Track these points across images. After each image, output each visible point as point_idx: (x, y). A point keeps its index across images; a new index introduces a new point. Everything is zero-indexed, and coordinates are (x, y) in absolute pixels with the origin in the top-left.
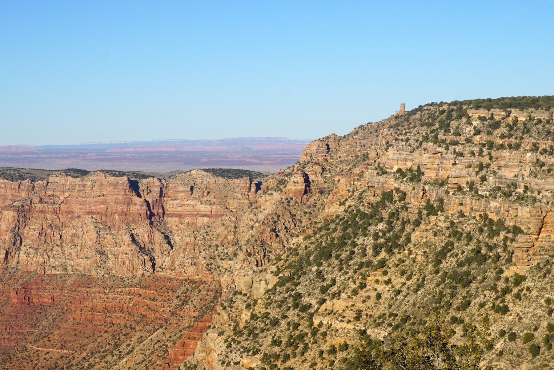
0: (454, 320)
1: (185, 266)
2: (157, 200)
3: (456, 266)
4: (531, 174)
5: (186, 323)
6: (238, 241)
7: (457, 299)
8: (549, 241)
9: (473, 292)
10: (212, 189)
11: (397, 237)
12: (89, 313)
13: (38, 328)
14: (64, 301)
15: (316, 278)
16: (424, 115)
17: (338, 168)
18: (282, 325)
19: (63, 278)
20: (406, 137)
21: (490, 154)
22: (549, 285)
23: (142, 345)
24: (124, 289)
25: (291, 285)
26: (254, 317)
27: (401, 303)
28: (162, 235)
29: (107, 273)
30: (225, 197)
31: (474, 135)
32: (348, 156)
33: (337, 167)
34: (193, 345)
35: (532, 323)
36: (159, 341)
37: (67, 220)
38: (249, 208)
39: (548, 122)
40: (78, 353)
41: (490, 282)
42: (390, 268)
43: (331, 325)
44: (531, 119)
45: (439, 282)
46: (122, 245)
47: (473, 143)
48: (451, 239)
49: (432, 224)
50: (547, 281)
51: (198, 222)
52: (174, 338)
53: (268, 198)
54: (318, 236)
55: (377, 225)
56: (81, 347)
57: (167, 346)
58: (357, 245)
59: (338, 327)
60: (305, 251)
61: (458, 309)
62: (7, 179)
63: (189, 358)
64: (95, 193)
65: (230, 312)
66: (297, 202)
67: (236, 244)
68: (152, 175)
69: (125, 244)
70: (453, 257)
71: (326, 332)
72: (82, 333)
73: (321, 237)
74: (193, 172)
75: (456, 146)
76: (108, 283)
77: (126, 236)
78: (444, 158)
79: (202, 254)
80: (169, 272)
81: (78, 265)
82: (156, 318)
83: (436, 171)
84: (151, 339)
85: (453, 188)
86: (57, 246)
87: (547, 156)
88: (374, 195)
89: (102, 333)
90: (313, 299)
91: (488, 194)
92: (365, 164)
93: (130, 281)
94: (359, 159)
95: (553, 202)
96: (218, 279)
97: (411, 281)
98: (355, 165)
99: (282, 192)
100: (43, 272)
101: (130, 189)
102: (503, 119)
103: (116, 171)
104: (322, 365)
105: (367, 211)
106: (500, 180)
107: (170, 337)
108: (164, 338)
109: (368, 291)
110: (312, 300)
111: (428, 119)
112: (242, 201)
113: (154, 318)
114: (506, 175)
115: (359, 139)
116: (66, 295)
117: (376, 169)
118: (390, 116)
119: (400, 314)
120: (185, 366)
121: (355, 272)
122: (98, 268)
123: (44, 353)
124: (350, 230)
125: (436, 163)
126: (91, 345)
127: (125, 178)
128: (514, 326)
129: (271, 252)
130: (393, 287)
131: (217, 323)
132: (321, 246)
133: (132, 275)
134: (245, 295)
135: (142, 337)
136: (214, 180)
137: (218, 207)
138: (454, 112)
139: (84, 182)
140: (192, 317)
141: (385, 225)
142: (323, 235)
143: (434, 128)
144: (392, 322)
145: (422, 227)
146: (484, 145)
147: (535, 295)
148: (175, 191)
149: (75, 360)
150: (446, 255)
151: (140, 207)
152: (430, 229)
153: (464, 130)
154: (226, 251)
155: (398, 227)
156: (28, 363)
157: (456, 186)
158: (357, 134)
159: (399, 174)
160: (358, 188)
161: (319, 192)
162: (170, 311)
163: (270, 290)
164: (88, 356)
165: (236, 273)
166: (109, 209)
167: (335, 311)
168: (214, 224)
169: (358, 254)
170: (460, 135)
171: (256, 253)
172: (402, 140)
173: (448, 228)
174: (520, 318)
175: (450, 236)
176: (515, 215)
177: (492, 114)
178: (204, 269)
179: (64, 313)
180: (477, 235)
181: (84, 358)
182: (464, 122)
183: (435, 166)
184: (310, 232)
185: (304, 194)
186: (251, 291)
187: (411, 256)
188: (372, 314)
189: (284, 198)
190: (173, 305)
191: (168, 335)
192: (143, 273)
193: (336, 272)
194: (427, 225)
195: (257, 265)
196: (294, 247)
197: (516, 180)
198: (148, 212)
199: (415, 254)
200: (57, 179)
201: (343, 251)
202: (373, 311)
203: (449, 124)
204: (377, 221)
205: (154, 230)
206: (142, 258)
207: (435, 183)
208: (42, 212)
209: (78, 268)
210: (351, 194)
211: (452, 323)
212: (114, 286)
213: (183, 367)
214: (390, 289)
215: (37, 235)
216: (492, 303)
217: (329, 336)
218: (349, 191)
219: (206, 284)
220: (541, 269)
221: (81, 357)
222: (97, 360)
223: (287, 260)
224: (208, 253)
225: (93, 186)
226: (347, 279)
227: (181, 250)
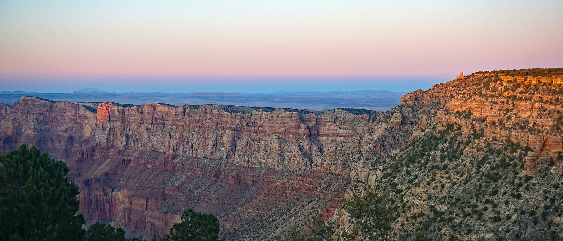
0: (488, 201)
1: (329, 165)
4: (538, 116)
5: (329, 197)
6: (361, 151)
7: (490, 189)
8: (547, 156)
9: (500, 184)
11: (456, 152)
13: (244, 198)
19: (259, 170)
20: (463, 92)
21: (513, 103)
22: (546, 182)
23: (303, 209)
27: (456, 190)
31: (504, 91)
33: (421, 109)
36: (313, 208)
38: (368, 132)
39: (550, 84)
40: (267, 213)
42: (450, 170)
44: (540, 82)
45: (479, 178)
46: (294, 152)
47: (503, 96)
48: (488, 153)
49: (476, 144)
50: (545, 180)
51: (338, 140)
53: (379, 126)
54: (408, 149)
57: (318, 211)
58: (431, 156)
59: (418, 203)
61: (490, 195)
62: (228, 112)
63: (330, 218)
66: (396, 129)
70: (488, 164)
71: (410, 206)
72: (269, 202)
73: (410, 150)
74: (336, 110)
75: (493, 98)
76: (285, 173)
77: (296, 147)
80: (321, 168)
81: (268, 163)
82: (312, 195)
83: (480, 113)
84: (309, 207)
85: (490, 123)
86: (256, 151)
88: (442, 126)
89: (281, 202)
94: (435, 105)
97: (462, 177)
99: (388, 123)
100: (248, 166)
102: (523, 82)
103: (291, 109)
105: (438, 135)
106: (519, 119)
107: (320, 206)
108: (316, 206)
109: (436, 182)
111: (477, 81)
115: (435, 93)
117: (444, 111)
118: (454, 79)
119: (455, 196)
120: (328, 223)
121: (429, 172)
123: (247, 213)
124: (427, 147)
125: (480, 108)
130: (451, 181)
135: (303, 205)
136: (348, 115)
137: (350, 131)
139: (272, 115)
140: (333, 194)
141: (448, 144)
142: (411, 149)
143: (480, 87)
146: (510, 98)
147: (537, 188)
148: (325, 121)
154: (353, 157)
157: (492, 122)
162: (320, 191)
163: (378, 180)
164: (272, 215)
165: (359, 170)
166: (287, 130)
167: (416, 194)
168: (347, 141)
170: (496, 91)
172: (460, 94)
174: (528, 201)
175: (487, 152)
176: (527, 140)
177: (516, 79)
178: (340, 167)
179: (259, 190)
180: (503, 151)
181: (270, 216)
185: (401, 124)
187: (463, 163)
188: (438, 196)
189: (389, 126)
190: (322, 187)
191: (318, 205)
192: (305, 169)
193: (418, 171)
195: (372, 166)
197: (529, 119)
200: (257, 113)
203: (489, 85)
204: (443, 142)
205: (312, 143)
206: (305, 159)
208: (248, 131)
210: (428, 125)
211: (486, 203)
212: (288, 175)
213: (326, 223)
214: (450, 182)
215: (245, 145)
216: (511, 192)
217: (412, 208)
218: (428, 123)
219: (342, 176)
221: (268, 215)
222: (277, 218)
224: (343, 157)
226: (424, 175)
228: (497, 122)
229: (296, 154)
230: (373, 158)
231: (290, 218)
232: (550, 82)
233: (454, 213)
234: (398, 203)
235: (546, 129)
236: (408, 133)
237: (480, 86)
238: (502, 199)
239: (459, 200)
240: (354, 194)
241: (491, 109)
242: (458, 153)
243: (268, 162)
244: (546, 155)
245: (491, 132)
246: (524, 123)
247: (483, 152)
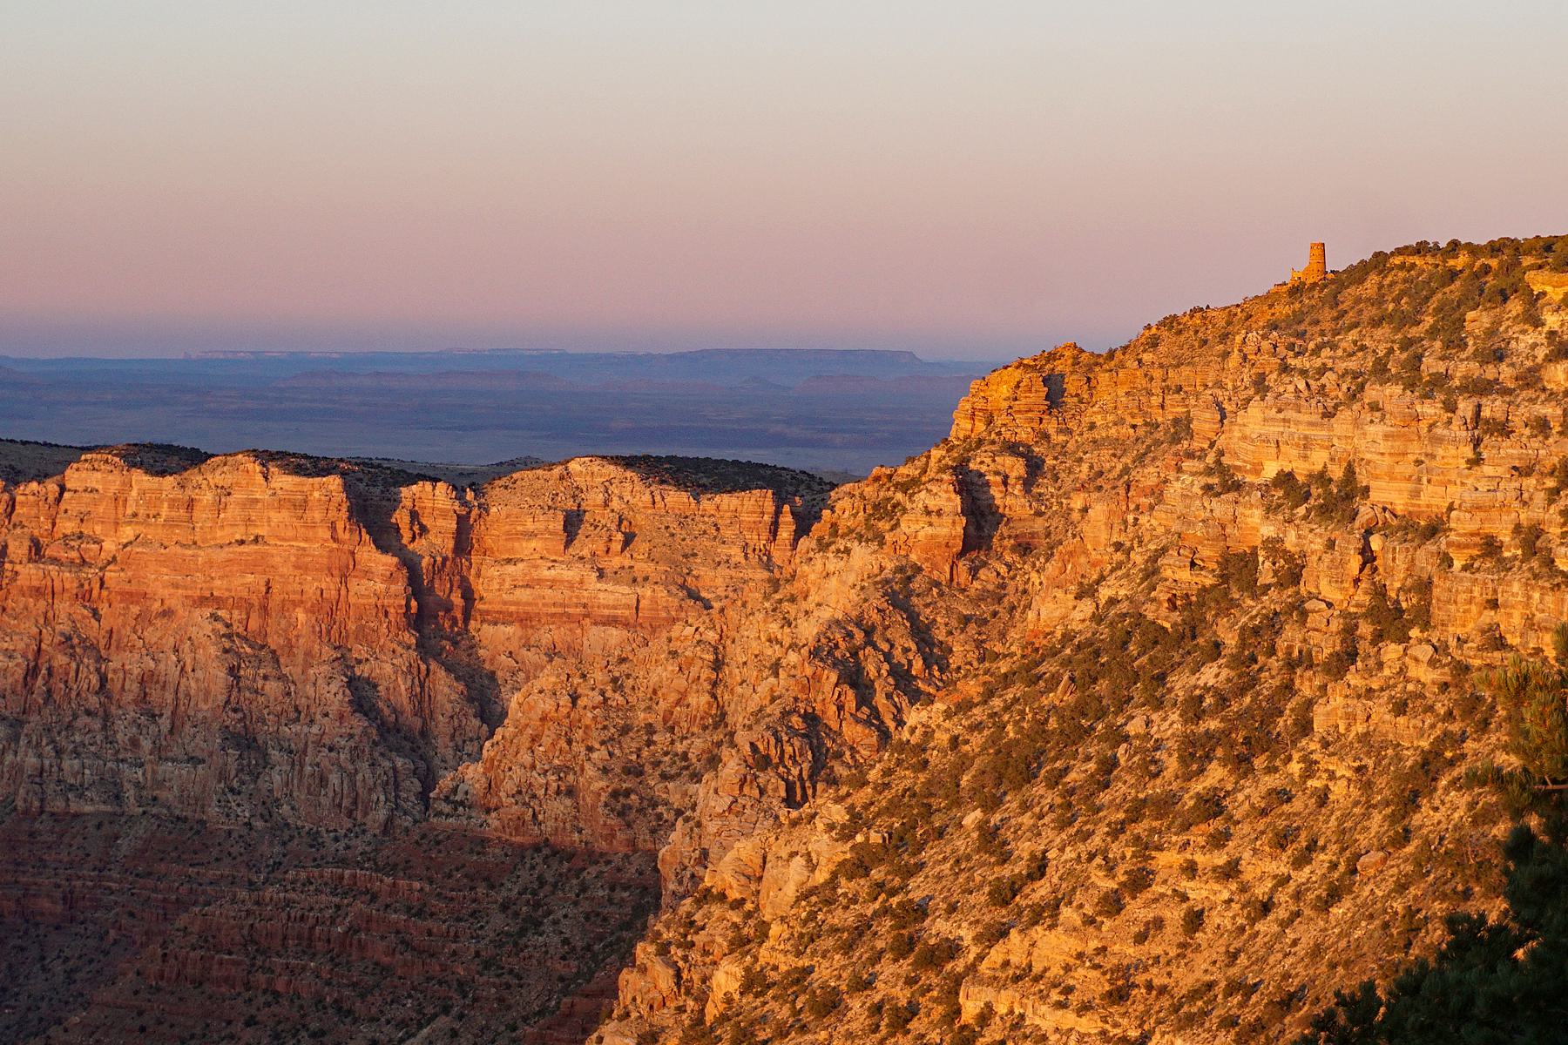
1: (534, 796)
2: (445, 559)
5: (531, 995)
6: (724, 715)
10: (641, 528)
12: (192, 954)
14: (108, 909)
15: (978, 851)
16: (1390, 285)
18: (850, 1014)
20: (1318, 362)
24: (316, 872)
25: (888, 873)
26: (754, 983)
27: (1270, 949)
28: (461, 687)
29: (262, 816)
30: (686, 556)
33: (1080, 460)
37: (124, 626)
38: (766, 597)
43: (1022, 1017)
46: (318, 717)
47: (1544, 390)
48: (1455, 727)
49: (1387, 672)
51: (586, 643)
53: (833, 564)
54: (997, 703)
58: (1126, 738)
60: (951, 757)
64: (227, 530)
65: (681, 964)
66: (938, 584)
67: (716, 727)
68: (431, 473)
69: (326, 715)
73: (1007, 708)
75: (1484, 401)
77: (334, 687)
78: (1439, 440)
79: (595, 755)
82: (428, 979)
83: (1410, 486)
88: (1193, 564)
90: (964, 925)
92: (1176, 454)
93: (341, 845)
94: (1159, 435)
96: (650, 846)
97: (1307, 869)
99: (882, 544)
101: (349, 519)
103: (306, 457)
105: (1166, 618)
109: (1155, 900)
110: (959, 927)
111: (1397, 300)
112: (749, 573)
117: (1209, 472)
118: (1272, 288)
122: (230, 796)
124: (1103, 686)
125: (1411, 458)
127: (334, 482)
129: (839, 755)
130: (1244, 889)
131: (634, 999)
132: (1001, 739)
133: (350, 825)
134: (738, 904)
136: (647, 497)
137: (661, 593)
138: (1489, 278)
141: (1225, 673)
142: (1016, 700)
143: (1414, 332)
145: (1352, 683)
148: (508, 533)
150: (1435, 779)
151: (383, 586)
152: (1382, 690)
153: (1513, 343)
154: (680, 748)
155: (1273, 677)
157: (1477, 539)
158: (1155, 345)
159: (1281, 493)
160: (1146, 539)
161: (1013, 550)
162: (478, 954)
163: (813, 891)
165: (712, 827)
166: (275, 589)
167: (1037, 969)
169: (1130, 770)
170: (1501, 359)
171: (787, 756)
172: (1303, 373)
173: (1444, 687)
175: (1450, 715)
183: (1407, 468)
184: (972, 688)
185: (961, 554)
186: (758, 892)
187: (1309, 783)
188: (1166, 981)
189: (890, 566)
192: (389, 821)
193: (1048, 833)
194: (1369, 673)
195: (790, 801)
196: (915, 739)
198: (414, 603)
199: (1325, 776)
200: (95, 479)
201: (1075, 759)
202: (1169, 974)
205: (433, 666)
206: (387, 764)
207: (1406, 528)
214: (1236, 898)
223: (887, 786)
224: (617, 752)
225: (219, 507)
226: (1084, 856)
227: (525, 740)
228: (1507, 539)
237: (1414, 329)
240: (678, 975)
241: (1476, 461)
242: (1284, 723)
247: (1428, 722)
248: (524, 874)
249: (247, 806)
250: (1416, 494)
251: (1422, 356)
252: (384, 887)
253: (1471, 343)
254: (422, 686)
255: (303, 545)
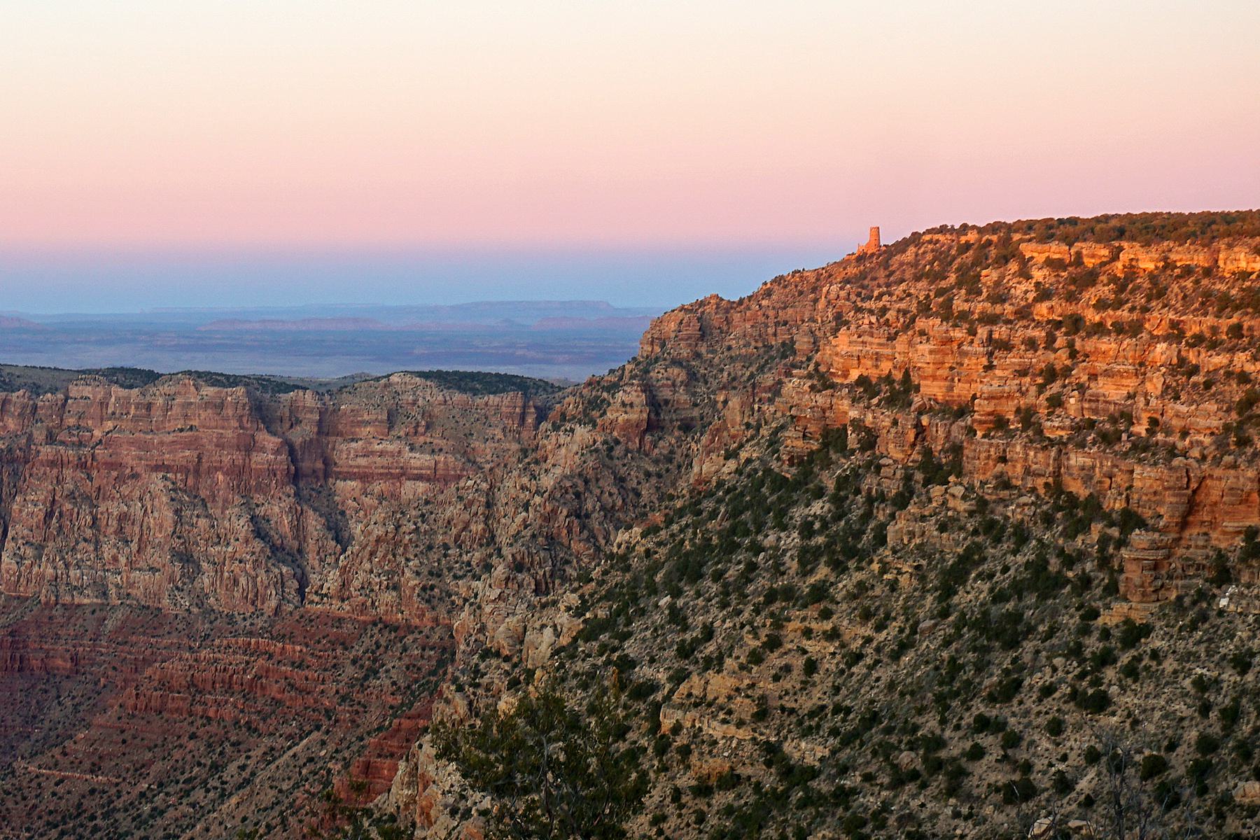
0: (983, 724)
1: (372, 590)
3: (989, 599)
5: (372, 718)
6: (493, 537)
7: (992, 675)
8: (1205, 547)
9: (1027, 658)
11: (858, 535)
13: (40, 725)
15: (669, 623)
17: (725, 374)
20: (881, 304)
21: (1071, 345)
22: (1203, 647)
23: (273, 766)
31: (1036, 300)
32: (747, 345)
33: (722, 370)
34: (389, 770)
35: (1163, 733)
38: (520, 461)
39: (1208, 272)
41: (1065, 637)
42: (838, 603)
43: (700, 729)
46: (232, 541)
47: (1034, 320)
48: (979, 539)
49: (934, 504)
51: (403, 492)
52: (346, 754)
54: (675, 527)
55: (808, 505)
56: (136, 770)
57: (329, 771)
58: (763, 550)
59: (717, 734)
60: (646, 562)
61: (992, 699)
63: (379, 799)
67: (488, 545)
69: (238, 540)
71: (688, 746)
72: (139, 739)
73: (681, 531)
74: (394, 379)
75: (994, 328)
76: (199, 625)
77: (242, 522)
79: (411, 564)
80: (336, 604)
81: (132, 585)
82: (306, 708)
83: (947, 383)
84: (294, 756)
85: (985, 422)
86: (85, 540)
87: (1203, 351)
88: (804, 436)
89: (184, 740)
91: (1066, 437)
94: (773, 353)
95: (1215, 456)
96: (447, 621)
97: (885, 632)
98: (763, 366)
99: (595, 425)
100: (53, 598)
102: (1103, 264)
103: (222, 375)
104: (679, 821)
105: (787, 472)
106: (1093, 405)
107: (337, 751)
109: (786, 653)
110: (658, 671)
111: (931, 263)
112: (506, 445)
113: (302, 708)
114: (1107, 393)
115: (774, 308)
116: (103, 650)
117: (810, 376)
121: (757, 611)
122: (176, 592)
123: (53, 782)
124: (747, 516)
125: (947, 365)
126: (158, 767)
128: (1121, 740)
130: (843, 646)
135: (272, 749)
136: (440, 398)
137: (451, 459)
139: (148, 398)
141: (827, 506)
142: (687, 526)
143: (943, 284)
144: (839, 724)
146: (1058, 325)
147: (1169, 669)
149: (122, 799)
151: (273, 457)
153: (1013, 291)
154: (465, 558)
156: (17, 803)
157: (991, 418)
159: (862, 390)
161: (680, 428)
162: (337, 692)
163: (562, 649)
164: (153, 790)
165: (488, 609)
167: (710, 697)
168: (441, 497)
170: (1004, 301)
172: (871, 312)
175: (976, 532)
176: (1127, 485)
177: (1079, 254)
179: (99, 693)
180: (1037, 531)
181: (142, 795)
182: (1012, 271)
183: (944, 372)
184: (658, 517)
185: (645, 432)
186: (521, 650)
187: (885, 577)
188: (793, 705)
189: (600, 439)
191: (331, 747)
193: (714, 611)
194: (922, 505)
195: (537, 592)
197: (1131, 405)
199: (895, 572)
201: (731, 562)
202: (796, 701)
204: (809, 495)
205: (305, 508)
206: (277, 571)
207: (944, 411)
208: (52, 464)
209: (133, 592)
210: (750, 433)
212: (212, 633)
214: (838, 651)
215: (42, 515)
216: (1070, 685)
217: (696, 754)
218: (748, 426)
219: (421, 632)
220: (1185, 610)
221: (136, 792)
222: (172, 800)
223: (603, 582)
225: (168, 408)
226: (738, 626)
228: (1012, 417)
229: (243, 551)
230: (540, 564)
231: (223, 803)
232: (1206, 265)
233: (855, 770)
234: (638, 736)
235: (1197, 442)
236: (675, 464)
238: (1039, 713)
239: (872, 719)
240: (470, 703)
241: (989, 367)
242: (868, 537)
243: (131, 581)
244: (1201, 543)
245: (989, 456)
246: (1113, 420)
247: (962, 536)
248: (367, 642)
249: (187, 599)
250: (951, 388)
251: (953, 299)
252: (277, 650)
253: (985, 290)
254: (298, 521)
255: (221, 431)
